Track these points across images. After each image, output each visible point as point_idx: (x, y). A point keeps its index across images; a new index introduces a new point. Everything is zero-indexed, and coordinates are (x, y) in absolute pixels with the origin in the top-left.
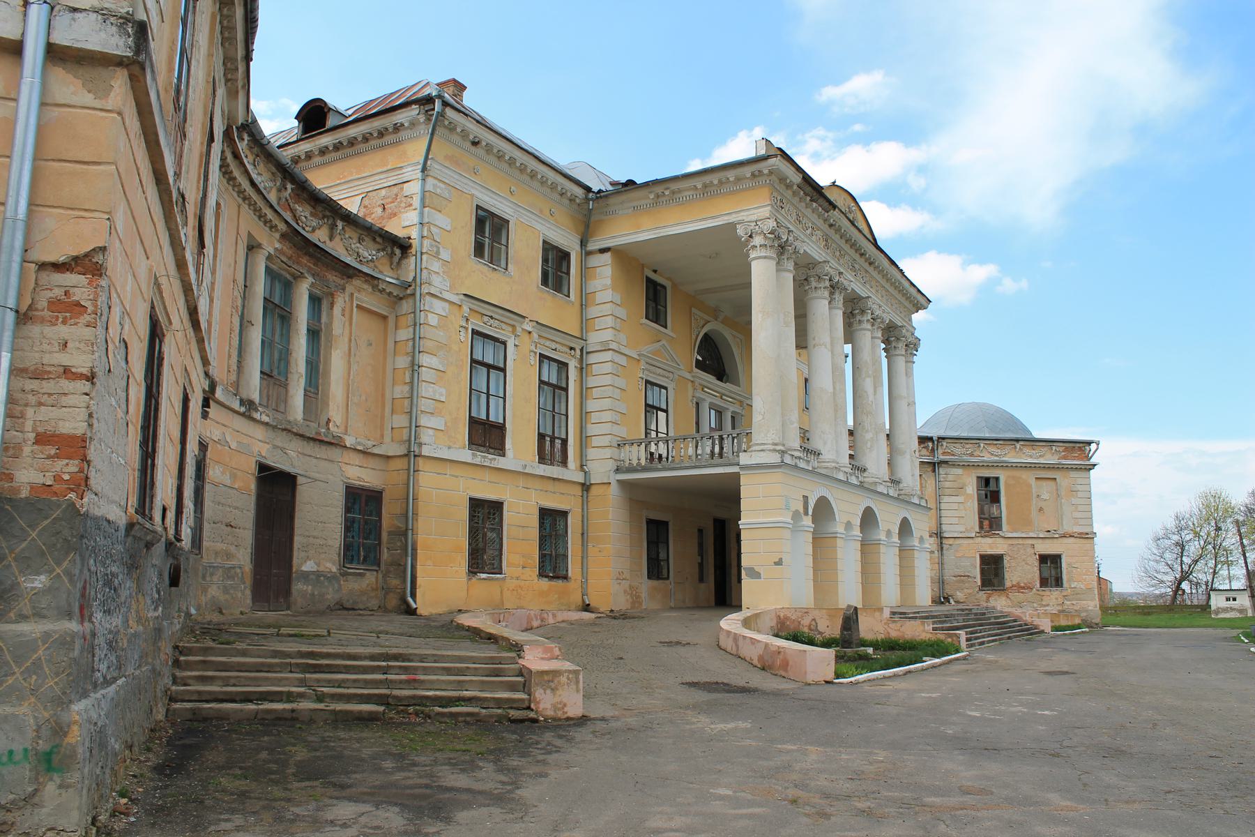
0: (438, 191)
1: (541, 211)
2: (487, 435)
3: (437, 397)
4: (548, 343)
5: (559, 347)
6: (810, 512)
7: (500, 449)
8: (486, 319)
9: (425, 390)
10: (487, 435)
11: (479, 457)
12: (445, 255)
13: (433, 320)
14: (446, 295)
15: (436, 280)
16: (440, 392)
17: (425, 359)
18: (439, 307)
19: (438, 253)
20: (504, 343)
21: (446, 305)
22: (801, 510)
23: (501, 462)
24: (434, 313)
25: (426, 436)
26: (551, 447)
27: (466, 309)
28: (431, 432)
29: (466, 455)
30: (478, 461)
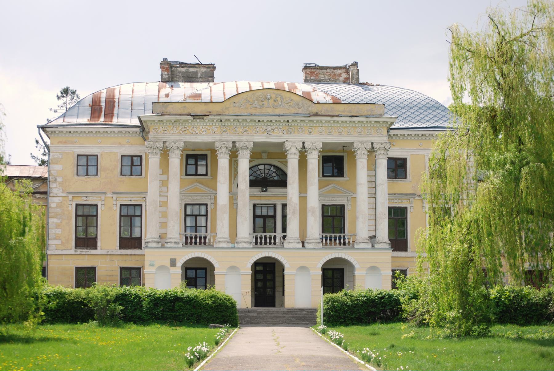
0: (55, 156)
1: (120, 144)
2: (86, 241)
3: (57, 233)
4: (127, 199)
5: (132, 199)
6: (179, 264)
7: (95, 247)
8: (83, 198)
9: (52, 231)
10: (86, 241)
11: (79, 251)
12: (59, 180)
13: (53, 205)
14: (59, 195)
15: (55, 191)
16: (59, 231)
17: (51, 220)
18: (56, 200)
19: (56, 180)
20: (97, 205)
21: (61, 198)
22: (168, 264)
23: (93, 252)
24: (54, 202)
25: (50, 248)
26: (130, 242)
27: (70, 197)
28: (54, 246)
29: (73, 251)
30: (78, 253)
